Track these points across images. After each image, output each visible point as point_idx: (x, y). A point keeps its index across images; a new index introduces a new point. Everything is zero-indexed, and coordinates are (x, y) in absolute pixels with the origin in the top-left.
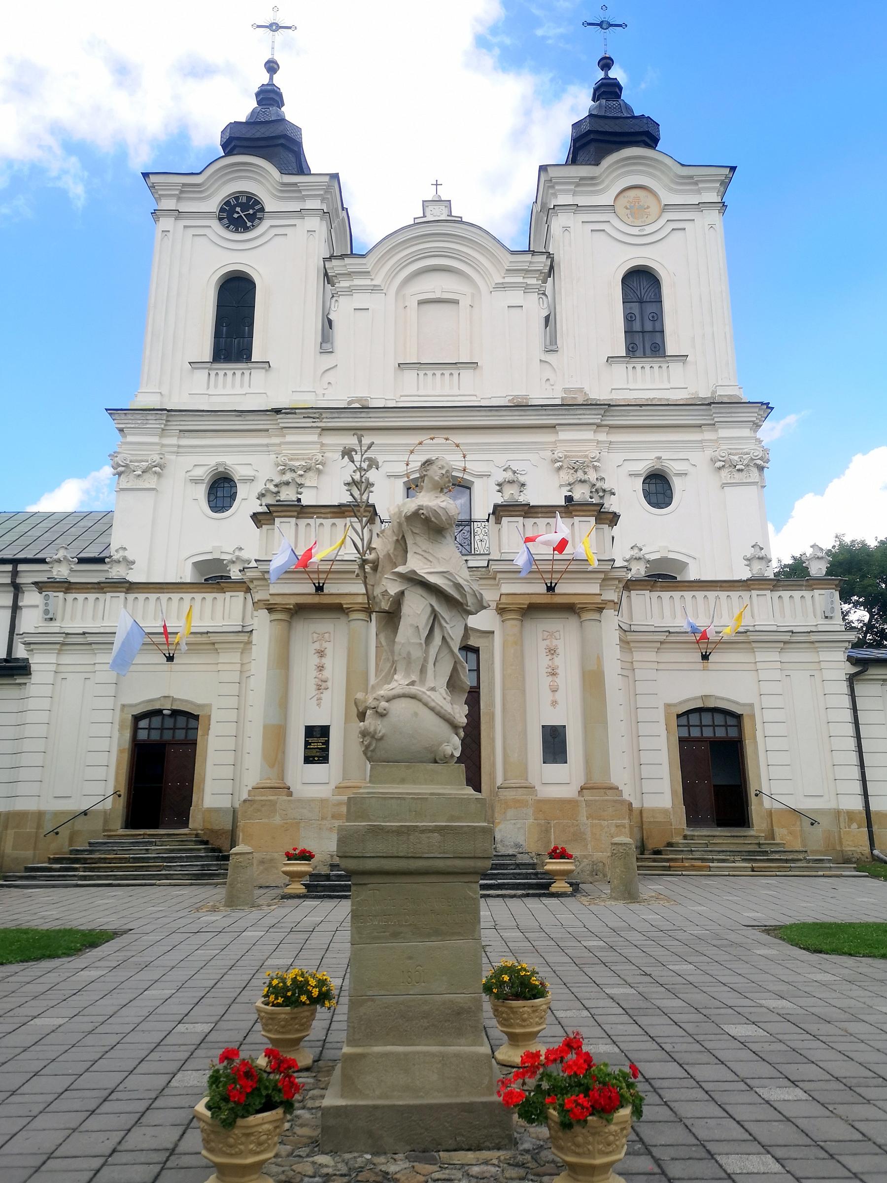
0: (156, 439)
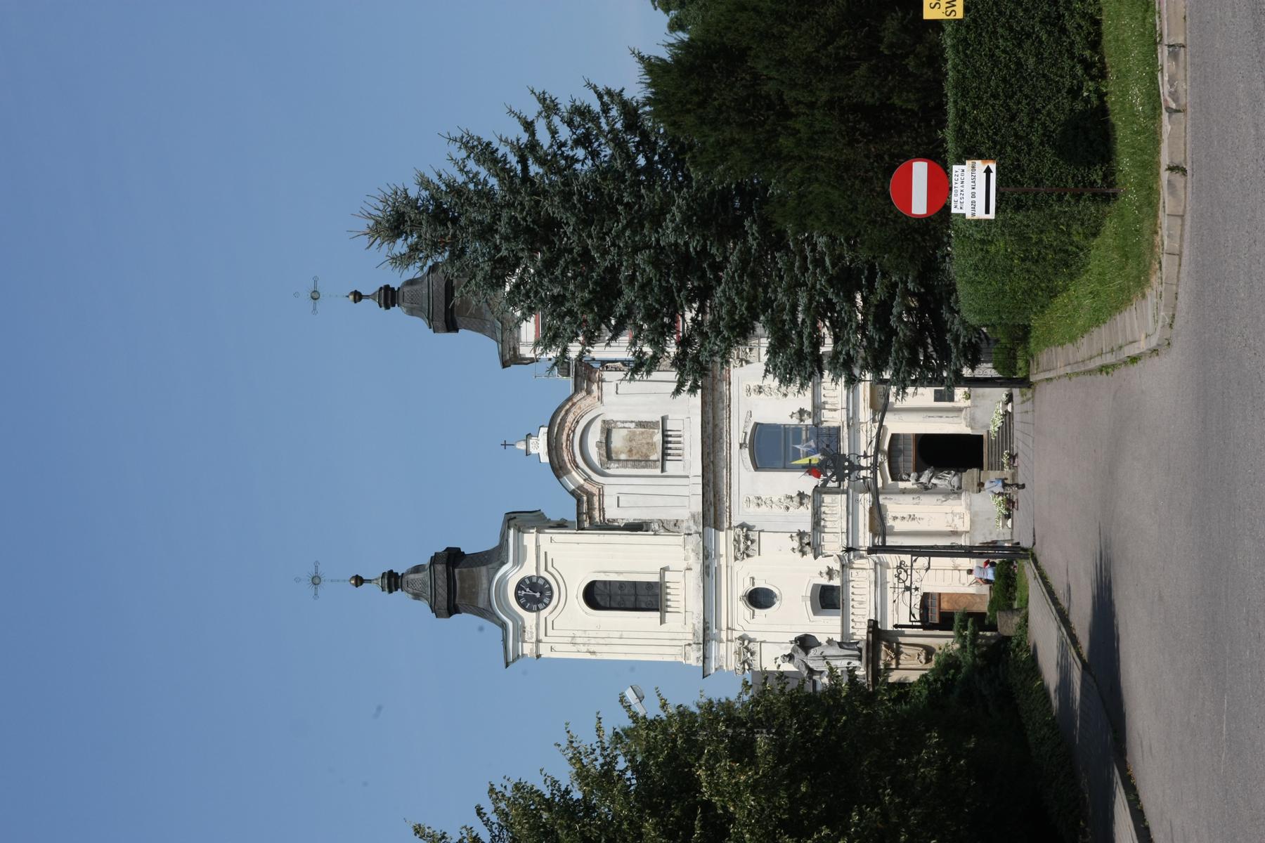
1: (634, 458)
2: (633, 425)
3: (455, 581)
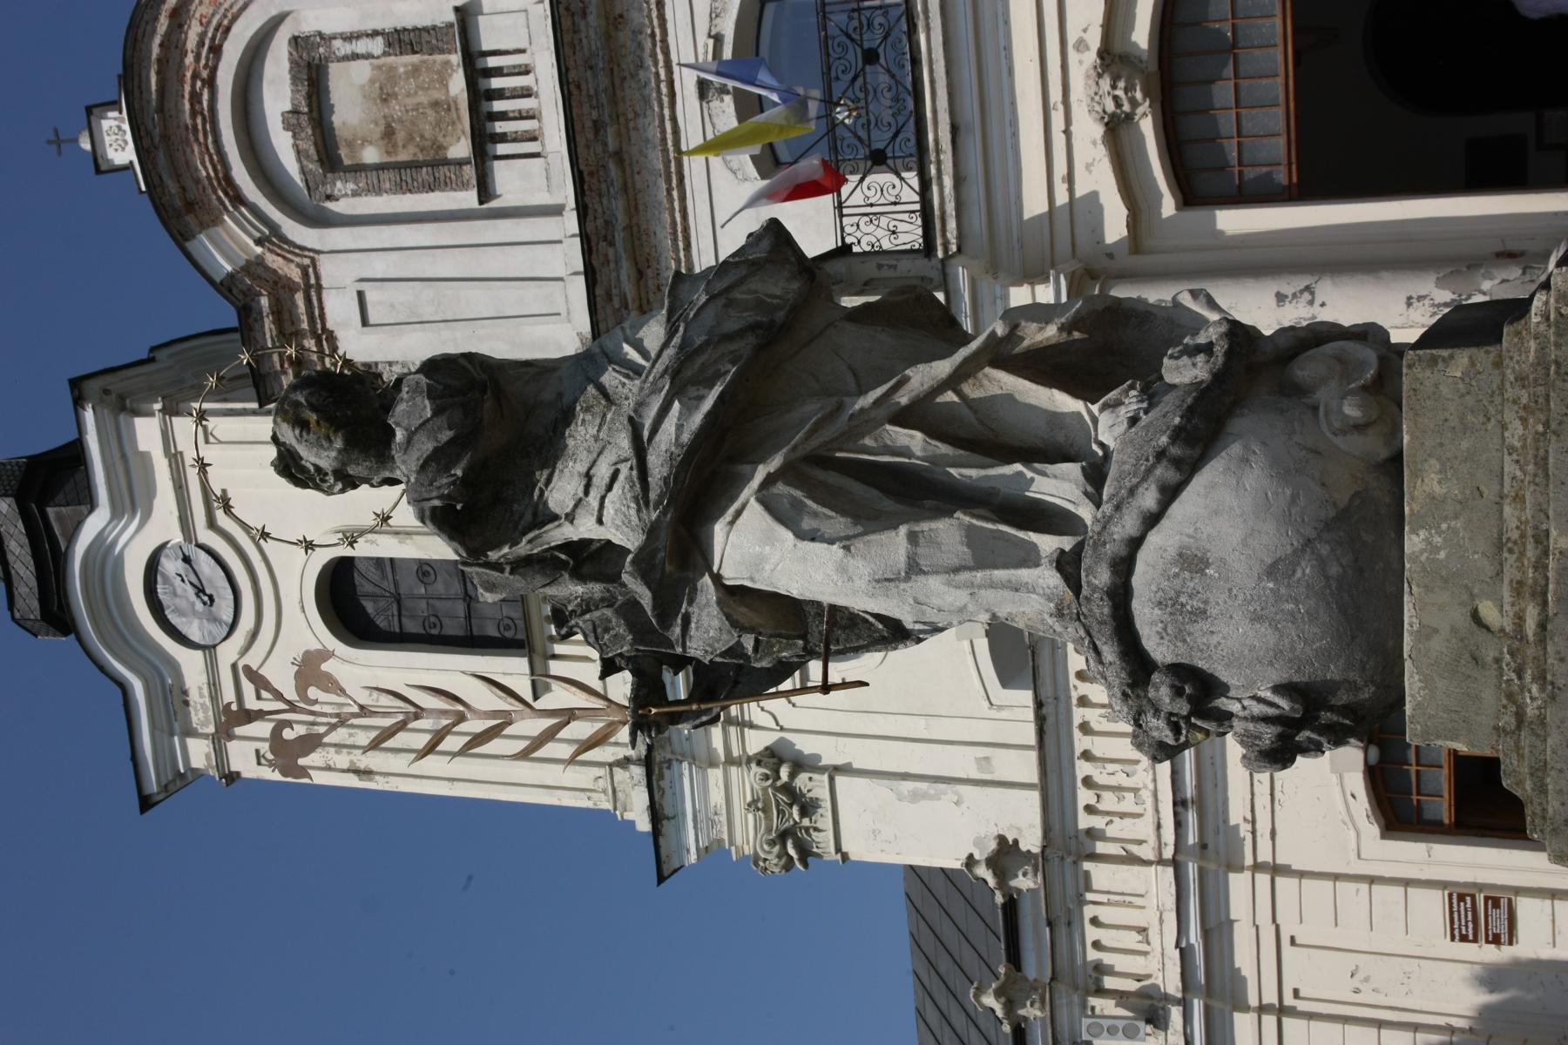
1: (403, 156)
2: (377, 46)
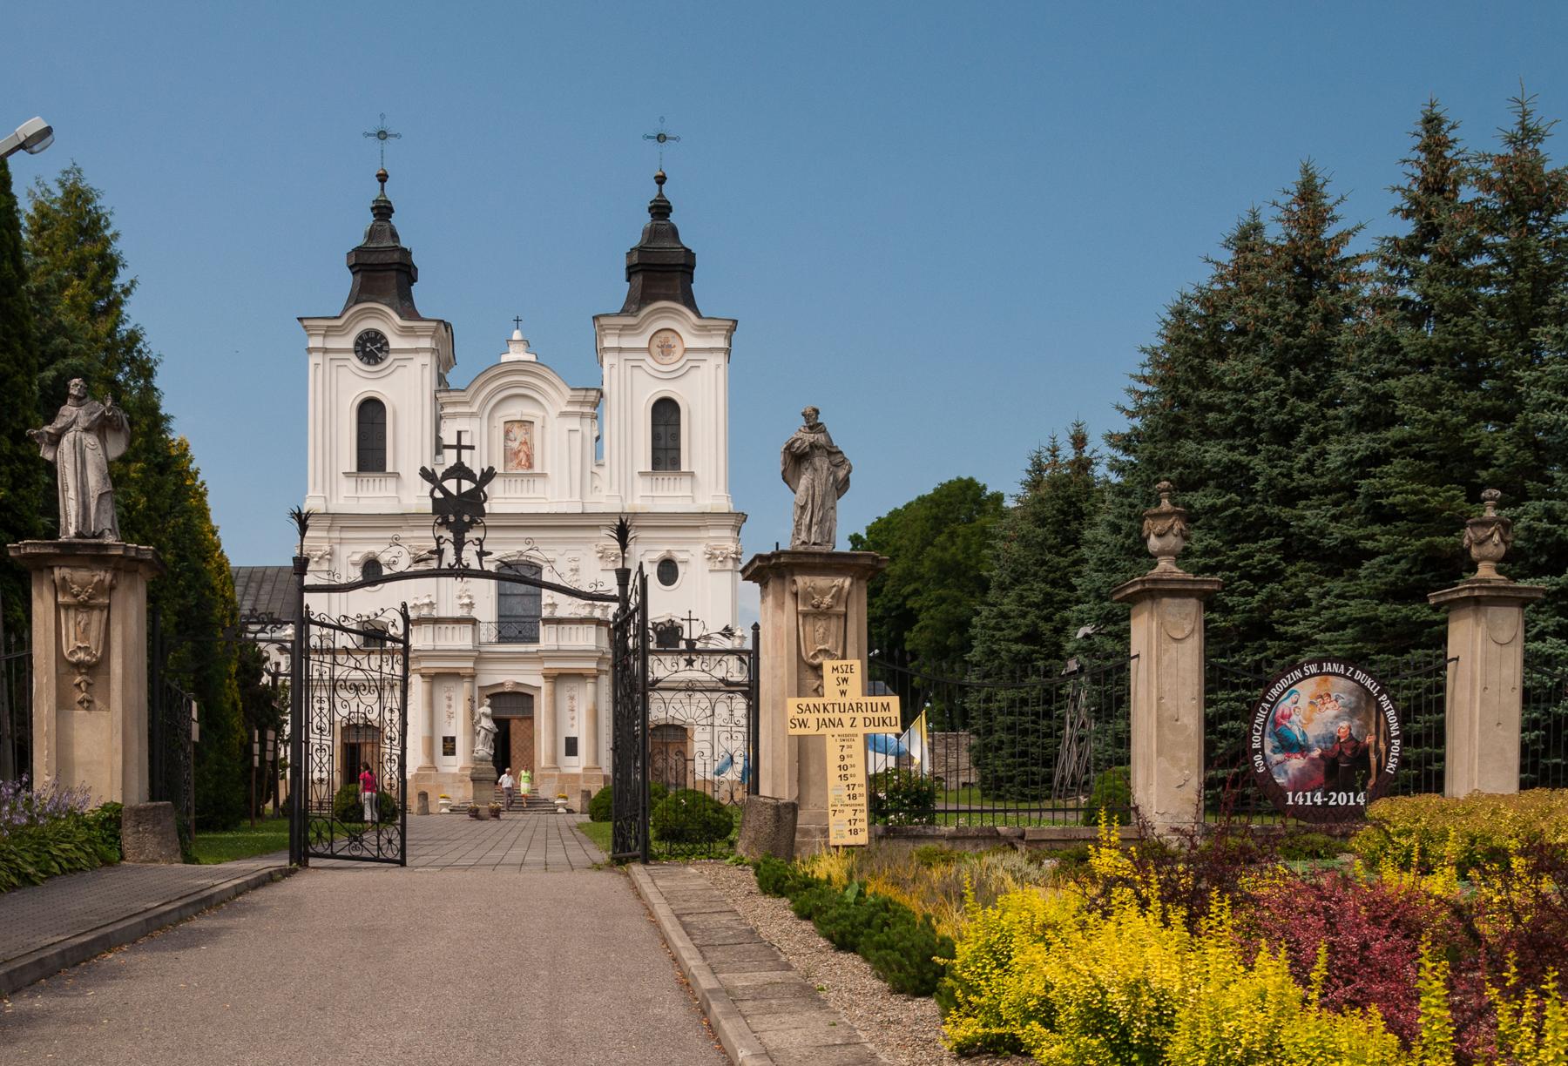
0: (324, 534)
3: (383, 271)
